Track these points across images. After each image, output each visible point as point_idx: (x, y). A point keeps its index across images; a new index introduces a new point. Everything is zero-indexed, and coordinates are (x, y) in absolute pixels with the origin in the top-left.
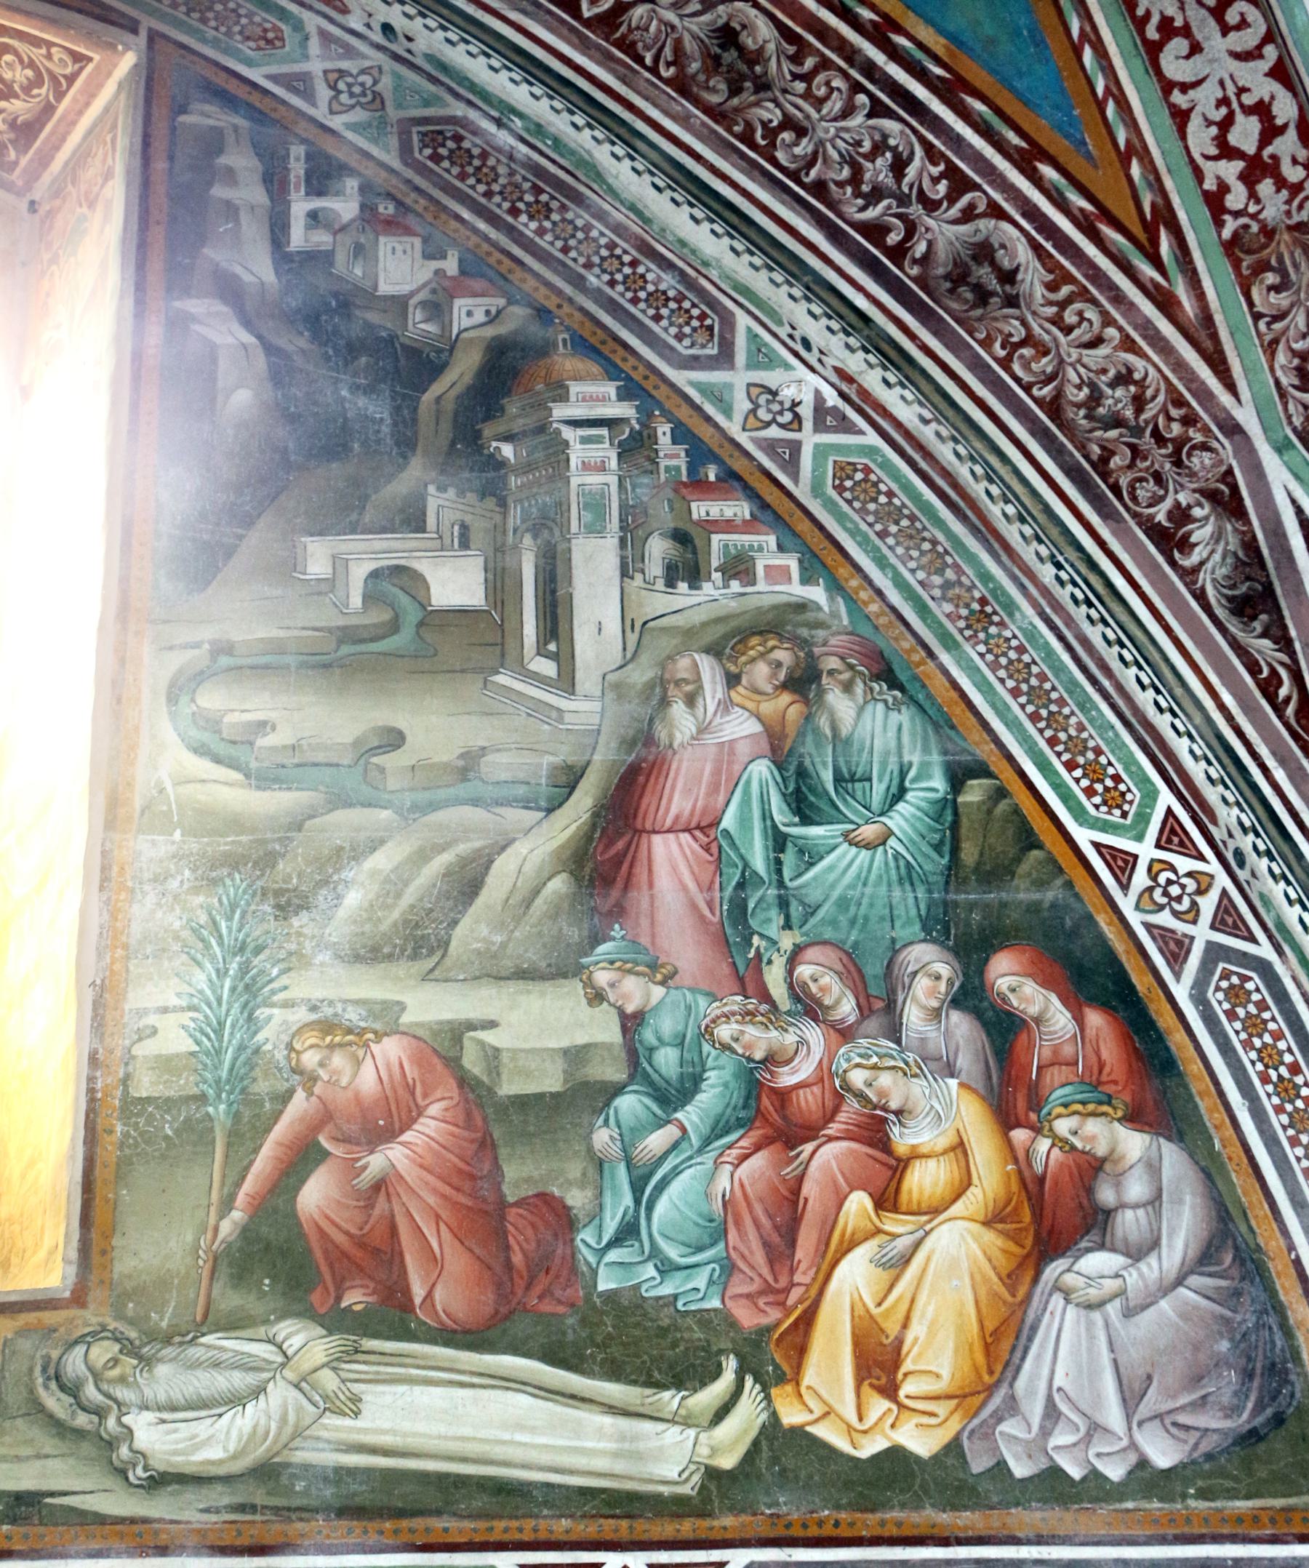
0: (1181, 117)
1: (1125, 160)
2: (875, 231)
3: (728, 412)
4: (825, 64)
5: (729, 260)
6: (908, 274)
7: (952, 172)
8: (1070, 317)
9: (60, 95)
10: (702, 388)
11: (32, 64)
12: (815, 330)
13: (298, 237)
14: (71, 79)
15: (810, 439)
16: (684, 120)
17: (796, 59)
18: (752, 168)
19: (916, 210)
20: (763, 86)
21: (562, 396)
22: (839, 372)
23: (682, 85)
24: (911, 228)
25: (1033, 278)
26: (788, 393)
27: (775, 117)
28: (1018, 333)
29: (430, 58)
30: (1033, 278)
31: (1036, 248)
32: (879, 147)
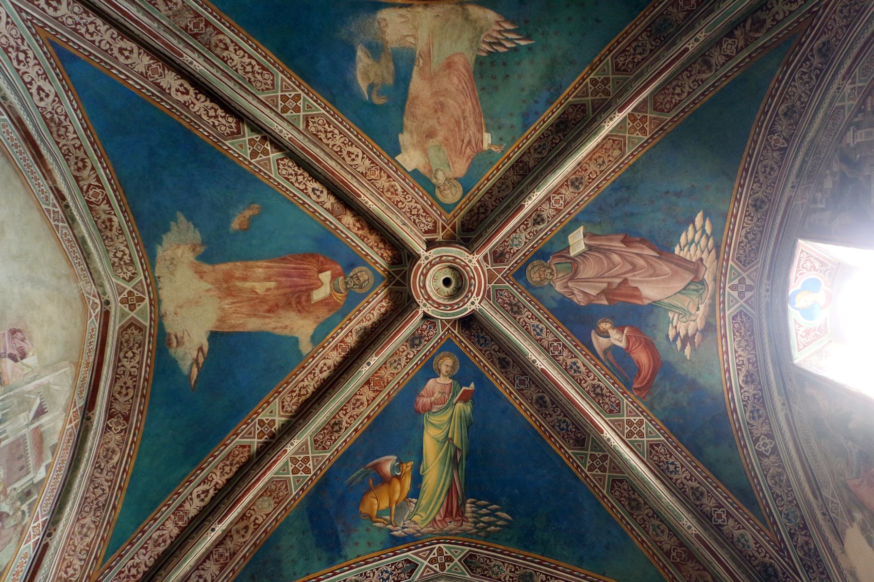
0: (791, 12)
1: (800, 23)
2: (817, 76)
3: (852, 105)
4: (787, 92)
5: (823, 109)
6: (825, 67)
7: (804, 61)
8: (830, 28)
9: (812, 256)
10: (849, 110)
11: (806, 261)
12: (835, 86)
13: (823, 206)
14: (808, 254)
15: (858, 84)
16: (803, 122)
17: (787, 99)
18: (809, 106)
19: (812, 68)
20: (793, 106)
21: (849, 144)
22: (844, 78)
23: (796, 124)
24: (816, 68)
25: (824, 39)
26: (849, 91)
27: (799, 102)
28: (834, 39)
29: (797, 178)
30: (824, 39)
31: (818, 39)
32: (801, 78)
